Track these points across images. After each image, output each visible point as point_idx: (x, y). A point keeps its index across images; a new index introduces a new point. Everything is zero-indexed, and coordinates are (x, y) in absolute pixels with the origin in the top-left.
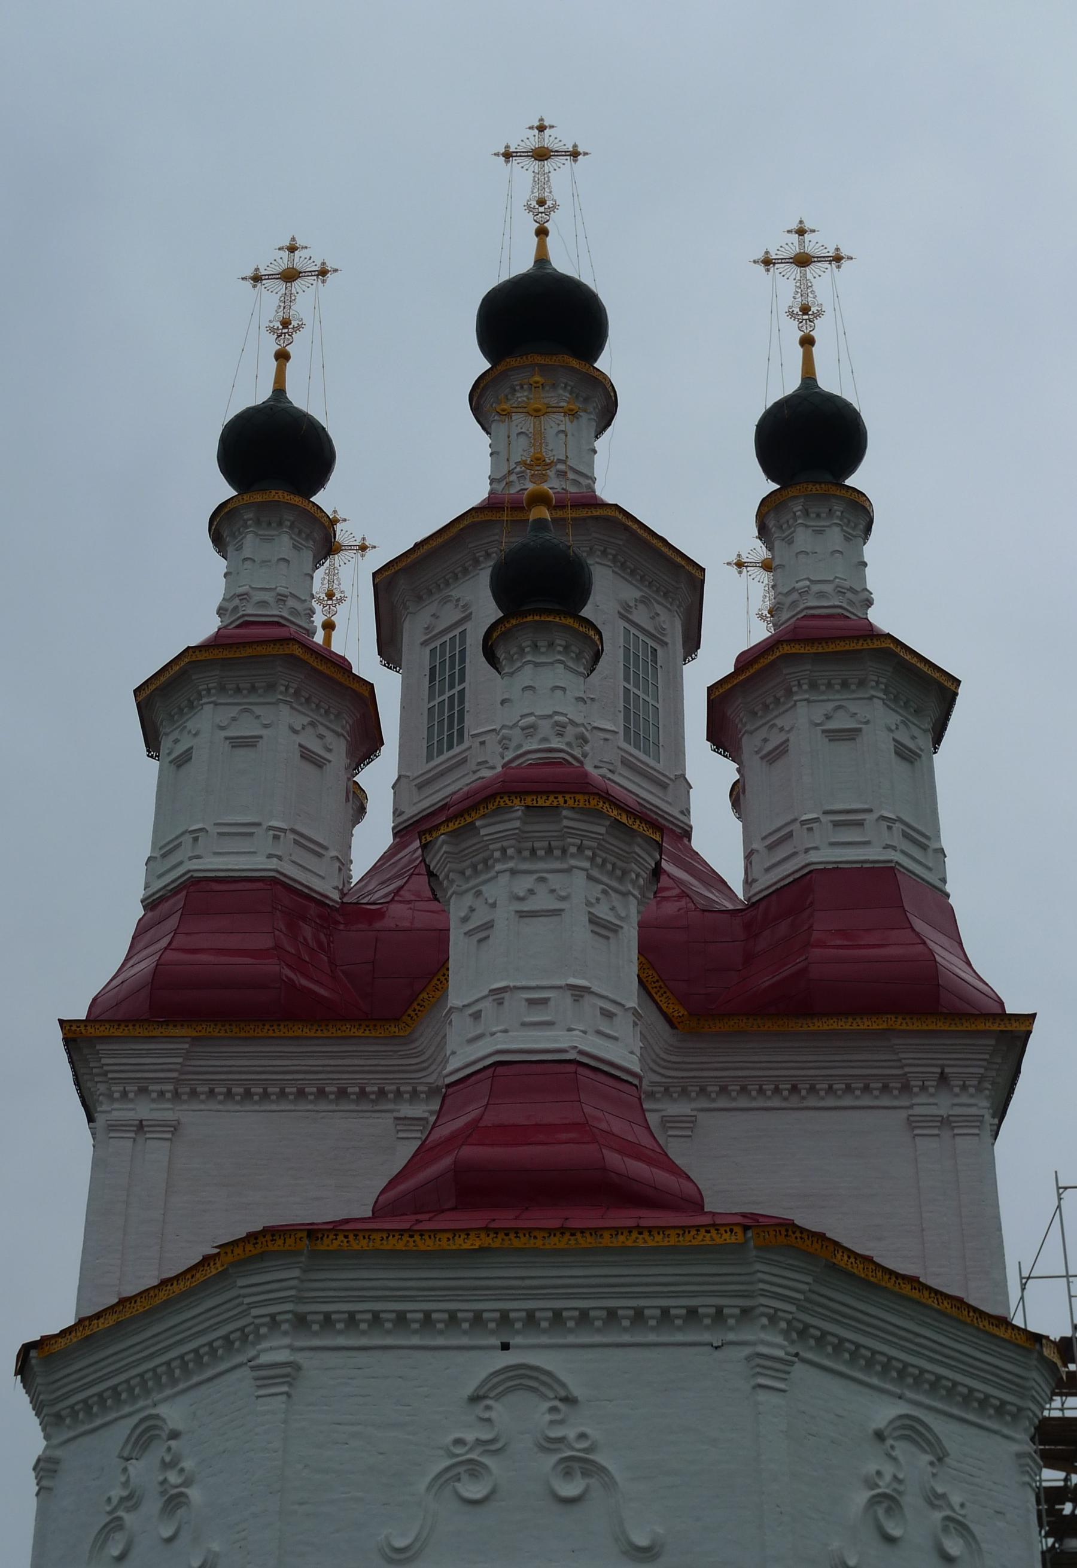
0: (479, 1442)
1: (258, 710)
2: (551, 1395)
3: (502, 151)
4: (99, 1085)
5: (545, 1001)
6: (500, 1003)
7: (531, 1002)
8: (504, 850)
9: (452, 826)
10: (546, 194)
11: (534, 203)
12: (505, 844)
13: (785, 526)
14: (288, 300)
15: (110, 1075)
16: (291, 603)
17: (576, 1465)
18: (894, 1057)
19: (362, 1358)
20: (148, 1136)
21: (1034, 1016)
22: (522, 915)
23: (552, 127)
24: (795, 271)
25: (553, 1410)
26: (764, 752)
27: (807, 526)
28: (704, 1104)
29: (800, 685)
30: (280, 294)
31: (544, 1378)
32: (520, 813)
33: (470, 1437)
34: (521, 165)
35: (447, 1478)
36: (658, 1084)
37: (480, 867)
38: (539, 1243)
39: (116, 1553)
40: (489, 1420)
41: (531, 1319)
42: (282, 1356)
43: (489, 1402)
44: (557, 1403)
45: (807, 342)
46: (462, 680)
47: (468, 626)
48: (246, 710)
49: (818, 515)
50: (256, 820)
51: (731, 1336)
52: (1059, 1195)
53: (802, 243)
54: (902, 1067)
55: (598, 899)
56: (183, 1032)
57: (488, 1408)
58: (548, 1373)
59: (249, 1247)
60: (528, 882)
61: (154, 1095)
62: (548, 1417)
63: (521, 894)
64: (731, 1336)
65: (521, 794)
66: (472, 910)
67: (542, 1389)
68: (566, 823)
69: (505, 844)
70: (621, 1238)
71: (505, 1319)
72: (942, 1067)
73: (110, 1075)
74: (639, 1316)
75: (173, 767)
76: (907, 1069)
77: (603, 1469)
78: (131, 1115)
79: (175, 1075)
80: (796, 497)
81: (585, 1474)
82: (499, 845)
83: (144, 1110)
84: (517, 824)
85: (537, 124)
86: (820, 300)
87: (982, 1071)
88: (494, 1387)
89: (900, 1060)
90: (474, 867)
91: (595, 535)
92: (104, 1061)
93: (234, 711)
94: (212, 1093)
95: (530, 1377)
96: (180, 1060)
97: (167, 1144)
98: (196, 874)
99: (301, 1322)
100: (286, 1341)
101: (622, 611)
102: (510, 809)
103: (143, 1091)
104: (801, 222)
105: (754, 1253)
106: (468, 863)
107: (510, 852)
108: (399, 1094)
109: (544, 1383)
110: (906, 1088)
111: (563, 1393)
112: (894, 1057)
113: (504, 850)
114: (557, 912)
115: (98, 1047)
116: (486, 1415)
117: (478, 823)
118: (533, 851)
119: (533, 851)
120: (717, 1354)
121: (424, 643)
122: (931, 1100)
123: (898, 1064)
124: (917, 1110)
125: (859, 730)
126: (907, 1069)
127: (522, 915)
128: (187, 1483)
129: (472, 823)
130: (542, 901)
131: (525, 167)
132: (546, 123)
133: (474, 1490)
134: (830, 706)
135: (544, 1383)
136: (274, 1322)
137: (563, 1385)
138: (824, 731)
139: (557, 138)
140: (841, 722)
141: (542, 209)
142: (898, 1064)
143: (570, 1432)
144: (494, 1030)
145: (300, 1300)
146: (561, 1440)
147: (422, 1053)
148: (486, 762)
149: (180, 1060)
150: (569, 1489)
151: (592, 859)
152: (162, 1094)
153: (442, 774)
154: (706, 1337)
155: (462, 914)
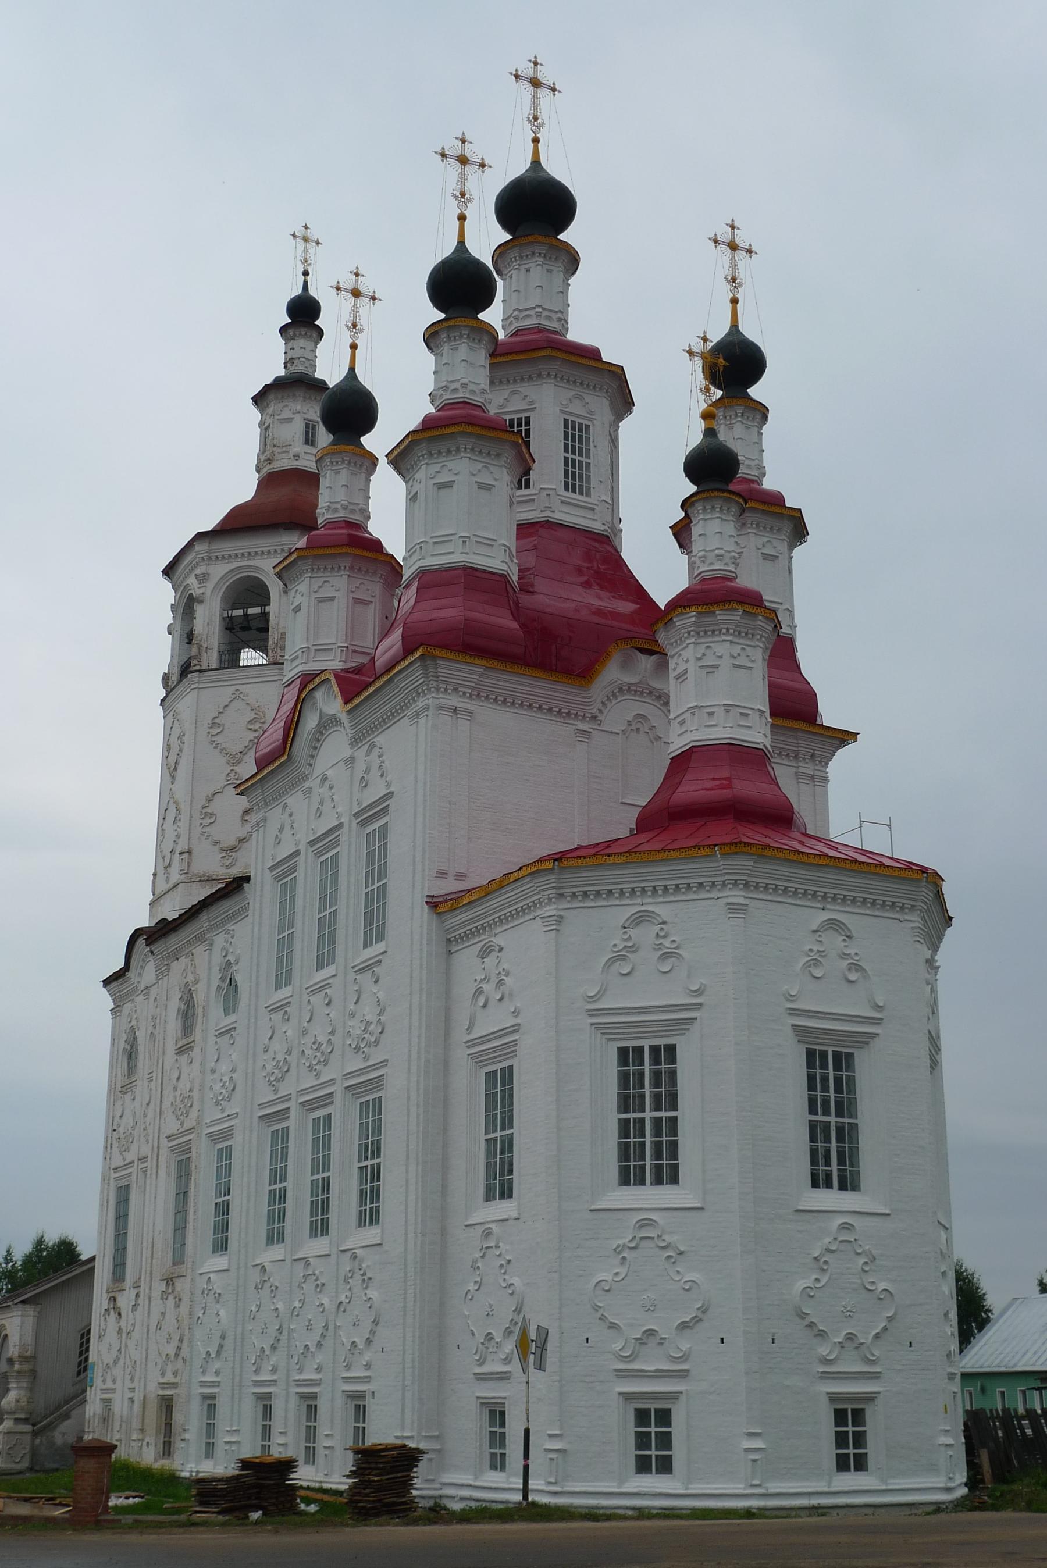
0: (819, 951)
1: (492, 468)
2: (843, 934)
4: (432, 682)
5: (747, 715)
6: (727, 711)
7: (741, 714)
8: (728, 629)
9: (700, 609)
12: (730, 627)
13: (728, 418)
14: (463, 178)
15: (441, 678)
16: (471, 387)
17: (853, 966)
18: (796, 742)
19: (770, 905)
20: (459, 716)
22: (735, 666)
25: (844, 940)
27: (743, 423)
29: (752, 524)
30: (458, 172)
31: (841, 925)
32: (740, 613)
33: (815, 948)
35: (807, 966)
37: (709, 633)
38: (848, 866)
40: (821, 941)
41: (834, 898)
42: (741, 900)
43: (820, 933)
44: (845, 938)
48: (485, 467)
49: (748, 418)
50: (495, 538)
51: (906, 917)
52: (861, 824)
53: (733, 234)
54: (798, 747)
56: (483, 662)
57: (820, 936)
58: (844, 924)
59: (733, 848)
60: (737, 649)
61: (461, 693)
62: (843, 944)
63: (735, 655)
64: (906, 917)
65: (742, 603)
66: (704, 655)
67: (840, 930)
68: (760, 623)
69: (730, 627)
70: (878, 869)
71: (825, 897)
72: (814, 750)
73: (441, 678)
74: (874, 903)
75: (435, 488)
76: (800, 749)
77: (865, 970)
78: (450, 703)
79: (473, 685)
80: (740, 405)
81: (857, 971)
82: (726, 626)
83: (454, 701)
84: (738, 618)
86: (742, 276)
88: (823, 927)
89: (798, 743)
90: (706, 632)
91: (606, 380)
92: (439, 670)
93: (480, 466)
94: (487, 697)
95: (836, 925)
96: (477, 677)
97: (469, 722)
98: (467, 564)
99: (747, 885)
100: (741, 893)
102: (736, 610)
103: (455, 690)
104: (733, 220)
105: (925, 884)
106: (703, 629)
107: (731, 631)
108: (576, 715)
109: (841, 928)
110: (796, 757)
111: (849, 934)
112: (796, 742)
113: (728, 629)
114: (751, 668)
115: (438, 662)
116: (820, 939)
117: (717, 612)
118: (740, 633)
119: (740, 633)
120: (901, 924)
122: (806, 766)
123: (797, 745)
124: (801, 770)
125: (777, 557)
126: (800, 749)
127: (735, 666)
128: (677, 948)
129: (713, 612)
130: (742, 661)
131: (527, 89)
133: (818, 973)
134: (766, 539)
135: (841, 928)
136: (736, 883)
137: (849, 930)
138: (762, 553)
140: (768, 550)
142: (797, 745)
143: (852, 952)
144: (727, 725)
145: (749, 875)
146: (849, 955)
147: (592, 697)
148: (550, 507)
149: (477, 677)
150: (853, 977)
152: (464, 693)
154: (897, 916)
155: (699, 656)
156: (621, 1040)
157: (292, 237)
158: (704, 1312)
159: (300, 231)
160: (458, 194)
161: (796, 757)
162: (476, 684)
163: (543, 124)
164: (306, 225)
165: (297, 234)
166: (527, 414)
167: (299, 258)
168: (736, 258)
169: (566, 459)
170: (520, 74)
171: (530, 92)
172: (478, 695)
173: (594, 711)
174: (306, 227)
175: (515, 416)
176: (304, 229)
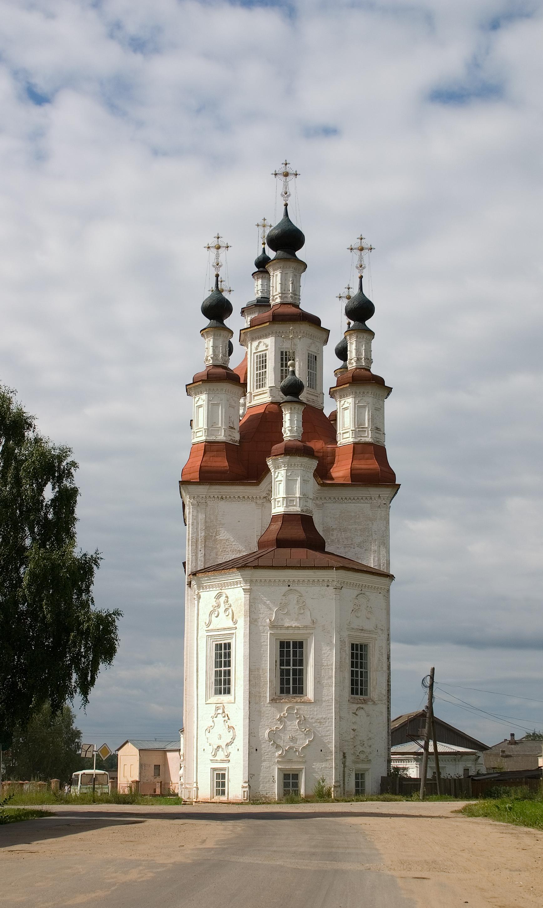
3: (274, 173)
10: (287, 190)
11: (283, 194)
21: (400, 485)
23: (289, 164)
24: (358, 252)
26: (343, 407)
28: (325, 501)
34: (280, 178)
36: (315, 497)
39: (216, 615)
45: (361, 277)
46: (265, 368)
47: (267, 352)
49: (360, 337)
53: (361, 243)
55: (305, 475)
79: (206, 493)
85: (285, 162)
86: (365, 263)
87: (388, 496)
101: (308, 349)
121: (255, 353)
132: (287, 162)
139: (291, 169)
141: (286, 196)
151: (304, 467)
152: (202, 497)
153: (260, 394)
156: (216, 641)
157: (256, 226)
158: (233, 740)
159: (260, 222)
160: (215, 264)
161: (371, 498)
162: (207, 493)
163: (289, 195)
164: (263, 220)
165: (259, 224)
166: (264, 353)
167: (260, 236)
168: (363, 255)
169: (282, 370)
170: (277, 173)
171: (283, 180)
172: (210, 496)
173: (264, 495)
174: (265, 220)
175: (261, 353)
176: (263, 221)
